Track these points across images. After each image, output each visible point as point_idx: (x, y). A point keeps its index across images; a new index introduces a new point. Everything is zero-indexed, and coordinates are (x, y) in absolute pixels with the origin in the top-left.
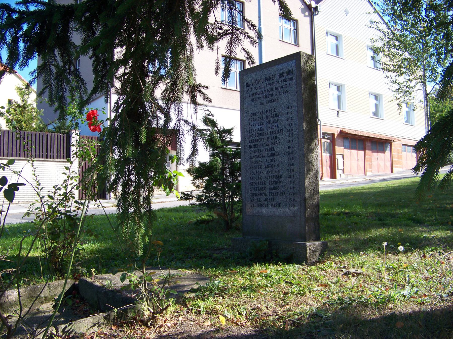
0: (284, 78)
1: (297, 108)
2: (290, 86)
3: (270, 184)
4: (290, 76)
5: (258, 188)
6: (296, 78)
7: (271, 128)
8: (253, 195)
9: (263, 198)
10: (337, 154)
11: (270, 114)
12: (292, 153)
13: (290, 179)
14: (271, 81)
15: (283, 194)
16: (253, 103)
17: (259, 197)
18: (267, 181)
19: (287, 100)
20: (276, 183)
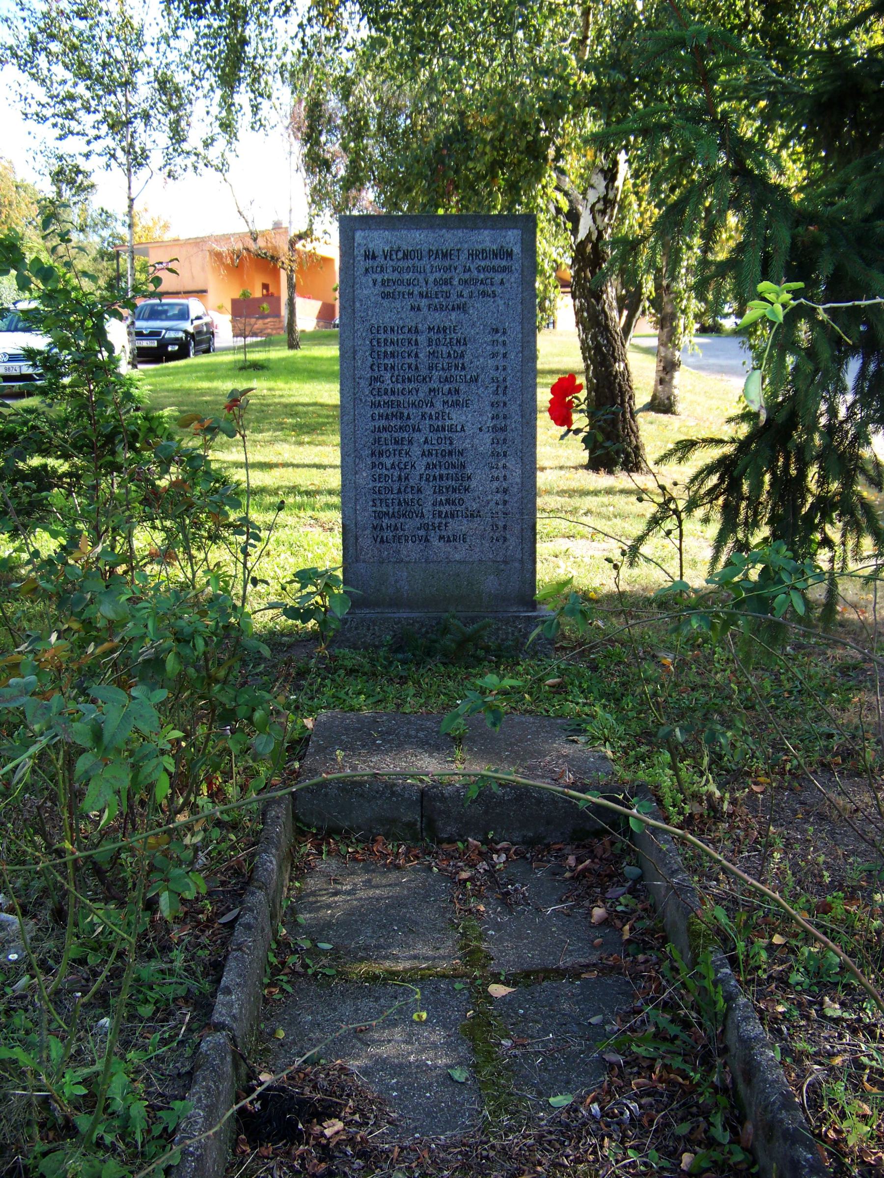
0: (487, 263)
1: (520, 336)
2: (502, 283)
3: (435, 493)
4: (504, 263)
5: (396, 502)
6: (522, 271)
7: (443, 369)
8: (379, 515)
9: (411, 525)
10: (335, 467)
11: (441, 336)
12: (503, 429)
13: (496, 484)
14: (447, 263)
15: (473, 515)
16: (386, 303)
17: (402, 520)
18: (428, 490)
19: (493, 313)
20: (454, 490)
